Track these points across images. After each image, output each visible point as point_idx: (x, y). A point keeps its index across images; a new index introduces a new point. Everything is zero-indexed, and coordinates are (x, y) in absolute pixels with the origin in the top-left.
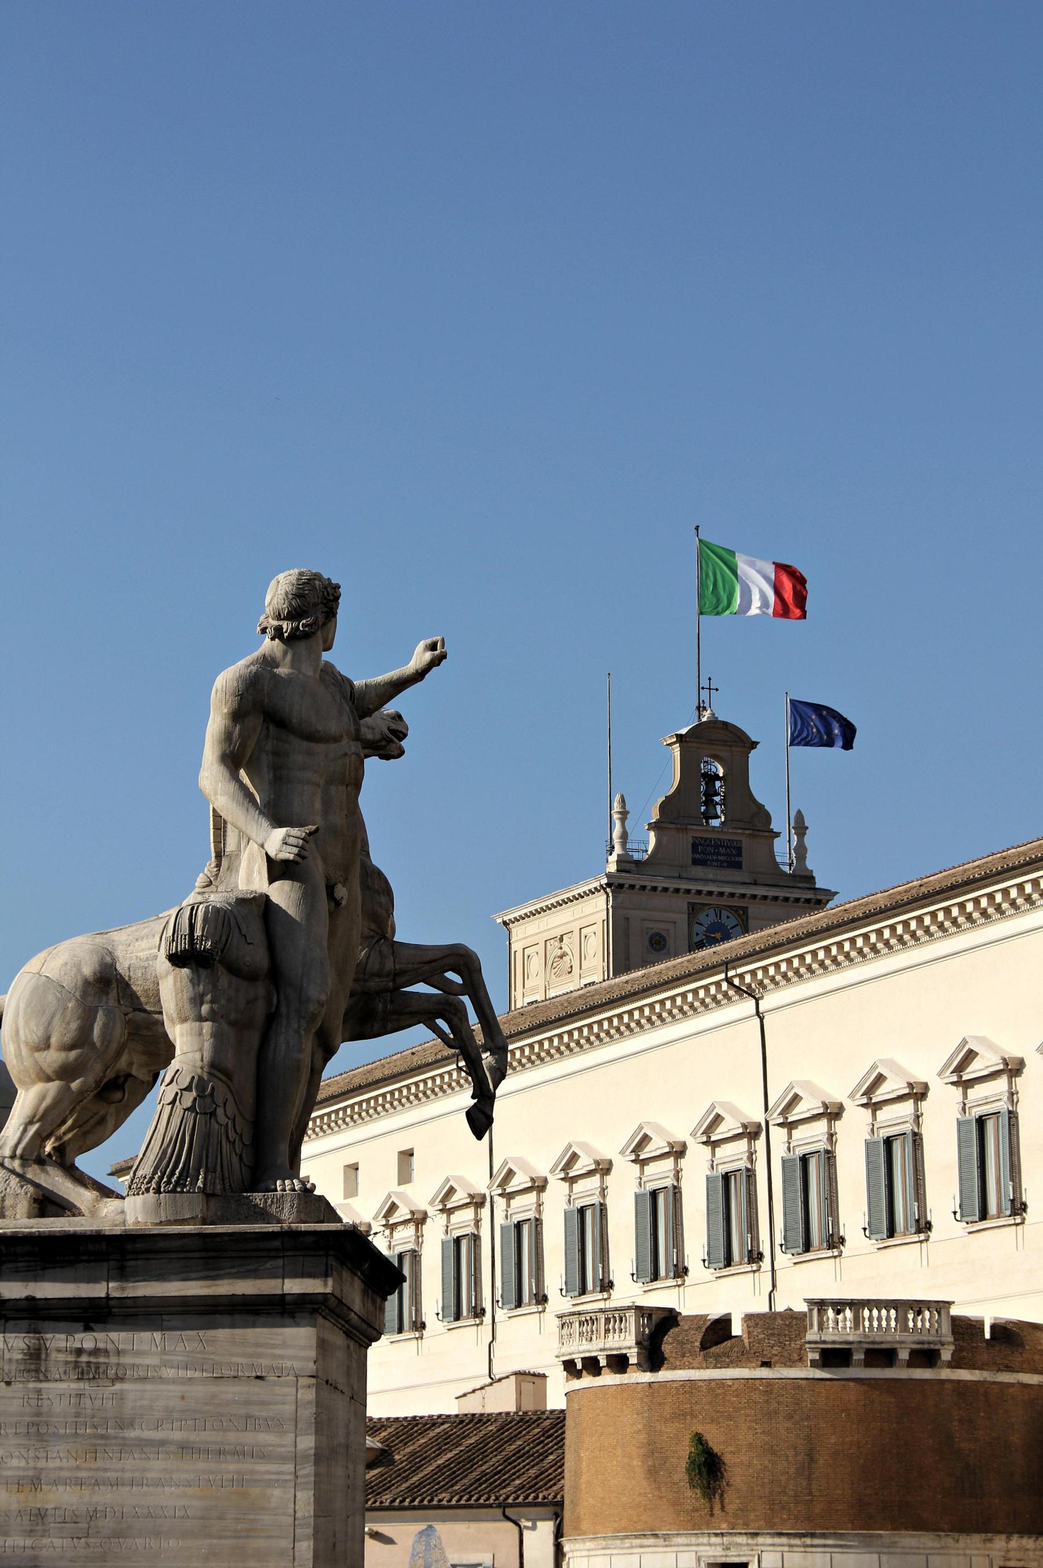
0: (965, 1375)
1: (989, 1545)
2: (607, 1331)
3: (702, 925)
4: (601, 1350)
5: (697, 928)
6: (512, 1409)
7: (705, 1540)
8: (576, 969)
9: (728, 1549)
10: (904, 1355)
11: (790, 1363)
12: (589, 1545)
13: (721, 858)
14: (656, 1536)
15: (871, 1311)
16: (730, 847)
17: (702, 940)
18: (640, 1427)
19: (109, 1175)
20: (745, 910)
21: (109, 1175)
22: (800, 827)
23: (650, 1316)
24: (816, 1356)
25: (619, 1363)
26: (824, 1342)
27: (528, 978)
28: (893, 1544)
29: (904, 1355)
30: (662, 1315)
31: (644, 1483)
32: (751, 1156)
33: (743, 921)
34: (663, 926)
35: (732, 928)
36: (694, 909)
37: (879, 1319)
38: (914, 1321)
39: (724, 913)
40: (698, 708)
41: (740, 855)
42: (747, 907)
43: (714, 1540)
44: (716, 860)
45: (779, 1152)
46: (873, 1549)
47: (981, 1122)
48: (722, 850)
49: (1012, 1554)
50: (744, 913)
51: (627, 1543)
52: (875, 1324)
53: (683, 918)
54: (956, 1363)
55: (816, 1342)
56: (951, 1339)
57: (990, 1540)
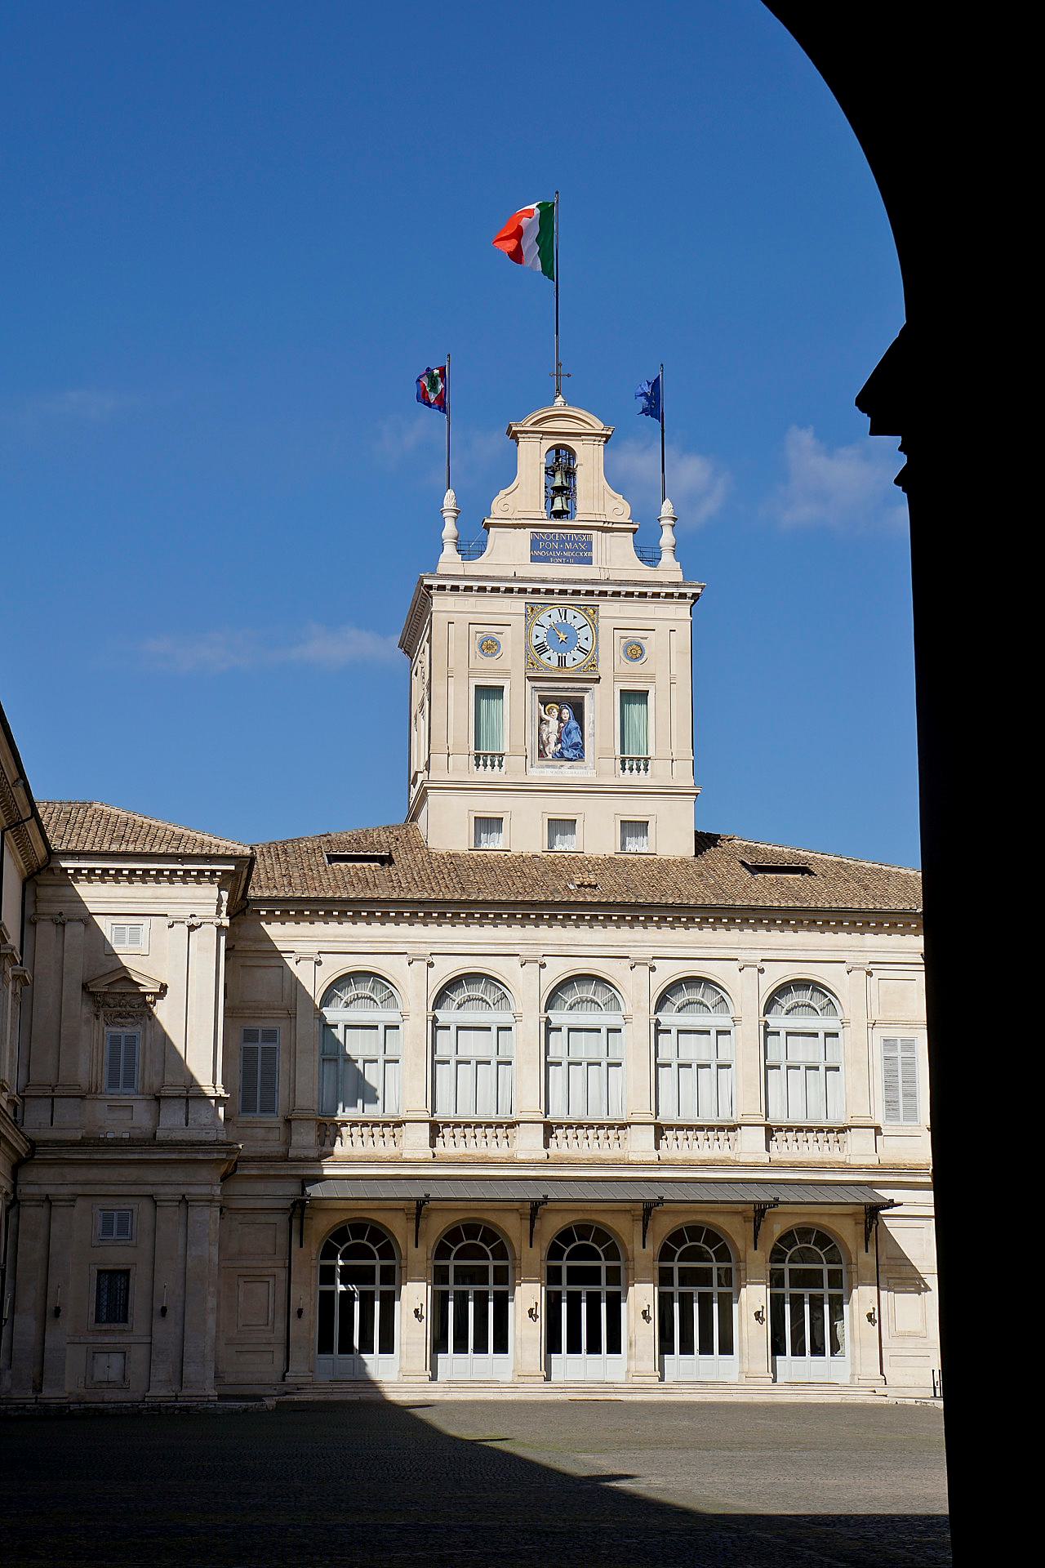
5: (537, 630)
16: (577, 542)
33: (593, 620)
35: (579, 629)
36: (532, 610)
44: (562, 556)
50: (594, 612)
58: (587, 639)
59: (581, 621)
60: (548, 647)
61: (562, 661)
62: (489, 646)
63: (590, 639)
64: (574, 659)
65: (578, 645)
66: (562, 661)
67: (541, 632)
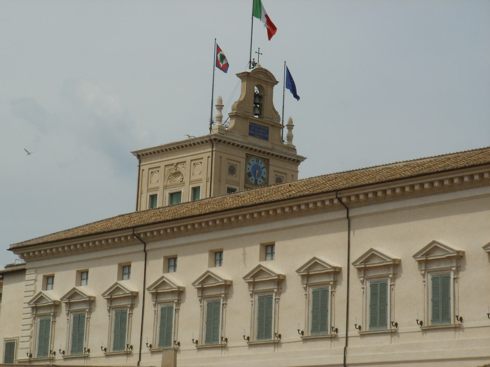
3: (251, 165)
5: (249, 166)
8: (186, 180)
13: (260, 134)
17: (250, 172)
19: (8, 250)
20: (268, 160)
21: (8, 250)
22: (290, 127)
27: (151, 183)
33: (267, 165)
34: (235, 163)
35: (262, 168)
36: (248, 156)
39: (260, 161)
40: (250, 62)
41: (268, 134)
42: (269, 159)
44: (258, 135)
48: (261, 131)
50: (267, 162)
53: (243, 161)
58: (264, 173)
59: (262, 165)
60: (252, 175)
61: (256, 181)
62: (232, 170)
63: (266, 173)
64: (260, 182)
65: (261, 175)
66: (256, 181)
67: (250, 167)
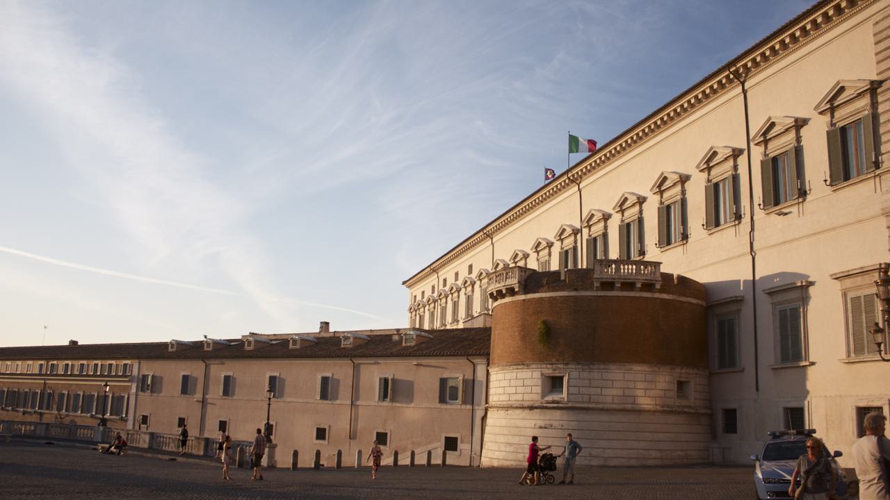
0: (665, 296)
1: (673, 371)
2: (506, 278)
4: (504, 286)
6: (482, 326)
7: (544, 366)
9: (555, 370)
10: (639, 285)
11: (587, 289)
12: (497, 369)
14: (524, 364)
15: (624, 265)
18: (519, 318)
23: (525, 272)
24: (599, 285)
25: (511, 291)
26: (602, 278)
28: (631, 369)
29: (639, 285)
30: (531, 272)
31: (520, 342)
32: (576, 242)
37: (628, 269)
38: (644, 271)
43: (549, 366)
45: (585, 236)
46: (621, 371)
47: (668, 207)
49: (682, 375)
51: (512, 368)
52: (626, 271)
54: (661, 291)
55: (598, 278)
56: (660, 279)
57: (674, 369)
